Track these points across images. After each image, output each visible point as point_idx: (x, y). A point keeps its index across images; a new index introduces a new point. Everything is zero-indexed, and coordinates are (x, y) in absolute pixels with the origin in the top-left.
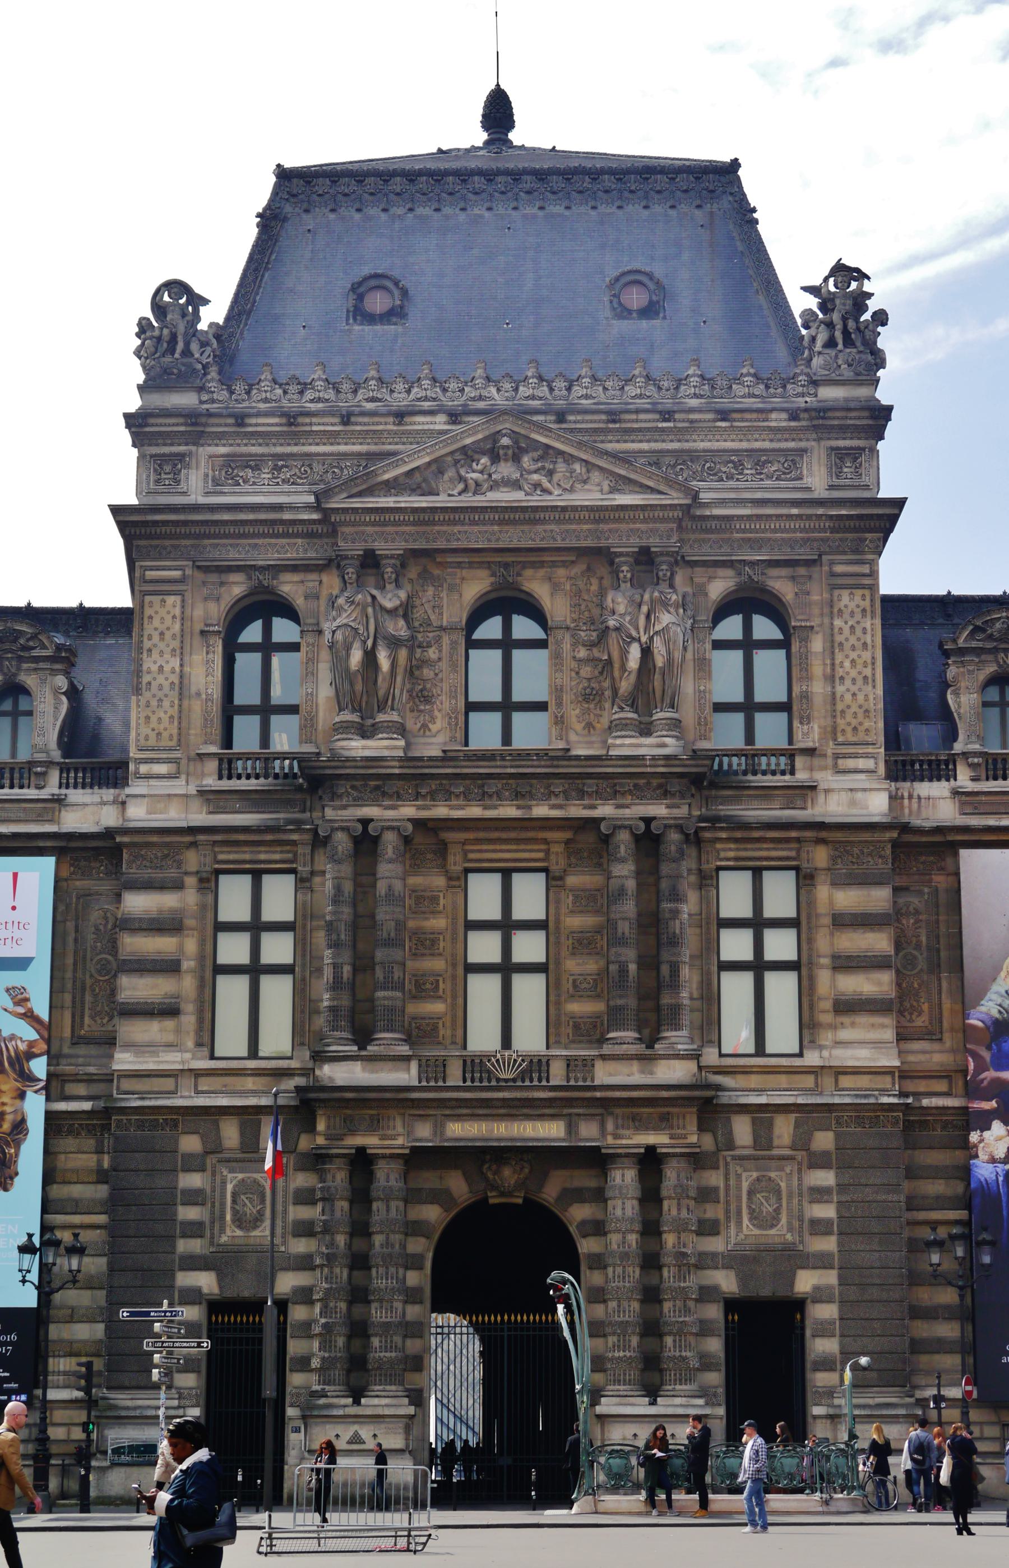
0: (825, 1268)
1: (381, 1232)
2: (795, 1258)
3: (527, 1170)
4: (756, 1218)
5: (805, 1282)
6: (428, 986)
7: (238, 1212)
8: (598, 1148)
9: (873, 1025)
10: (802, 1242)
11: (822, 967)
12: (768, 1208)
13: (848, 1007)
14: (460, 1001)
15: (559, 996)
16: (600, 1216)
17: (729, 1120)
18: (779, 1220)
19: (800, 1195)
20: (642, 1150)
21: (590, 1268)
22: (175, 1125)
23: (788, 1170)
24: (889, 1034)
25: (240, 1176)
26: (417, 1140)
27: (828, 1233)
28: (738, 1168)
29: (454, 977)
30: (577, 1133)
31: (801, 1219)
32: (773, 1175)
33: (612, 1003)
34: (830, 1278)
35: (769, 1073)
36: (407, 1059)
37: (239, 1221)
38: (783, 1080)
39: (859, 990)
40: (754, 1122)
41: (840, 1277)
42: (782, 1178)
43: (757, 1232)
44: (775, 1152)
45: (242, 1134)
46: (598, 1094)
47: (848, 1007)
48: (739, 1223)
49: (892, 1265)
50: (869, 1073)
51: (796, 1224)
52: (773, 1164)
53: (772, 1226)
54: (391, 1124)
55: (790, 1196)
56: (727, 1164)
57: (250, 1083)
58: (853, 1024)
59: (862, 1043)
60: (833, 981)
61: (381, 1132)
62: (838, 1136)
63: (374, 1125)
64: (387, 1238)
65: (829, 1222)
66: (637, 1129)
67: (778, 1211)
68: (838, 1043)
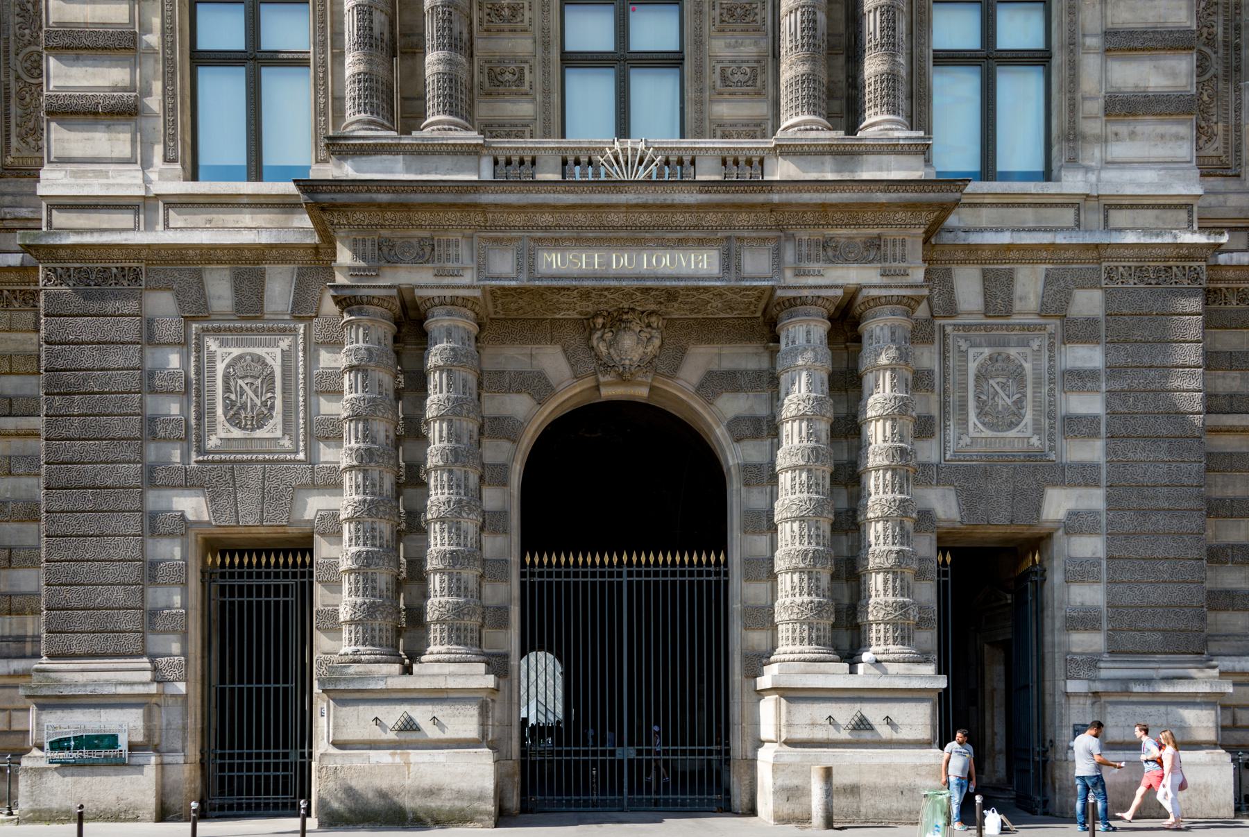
0: (1086, 485)
2: (1043, 470)
3: (657, 342)
4: (986, 415)
5: (1057, 504)
6: (508, 76)
7: (233, 404)
9: (1162, 137)
10: (1052, 448)
11: (1087, 51)
12: (1004, 400)
13: (1125, 107)
14: (556, 98)
15: (701, 91)
16: (762, 411)
17: (948, 273)
18: (1020, 417)
19: (1051, 381)
21: (747, 484)
22: (136, 275)
23: (1035, 345)
24: (1185, 150)
25: (236, 351)
27: (1095, 435)
28: (962, 342)
29: (546, 63)
31: (1051, 416)
32: (1013, 352)
34: (1095, 499)
35: (1007, 205)
37: (234, 420)
38: (1028, 216)
39: (1142, 84)
40: (985, 273)
41: (1109, 499)
42: (1027, 359)
43: (988, 433)
44: (1015, 320)
45: (237, 290)
47: (1125, 107)
48: (964, 422)
49: (1186, 481)
50: (1154, 207)
51: (1046, 423)
52: (1014, 335)
53: (1011, 425)
55: (1038, 383)
56: (945, 336)
57: (246, 218)
58: (1133, 135)
59: (1145, 163)
60: (1104, 70)
62: (1109, 296)
65: (1093, 420)
67: (1019, 403)
68: (1109, 164)
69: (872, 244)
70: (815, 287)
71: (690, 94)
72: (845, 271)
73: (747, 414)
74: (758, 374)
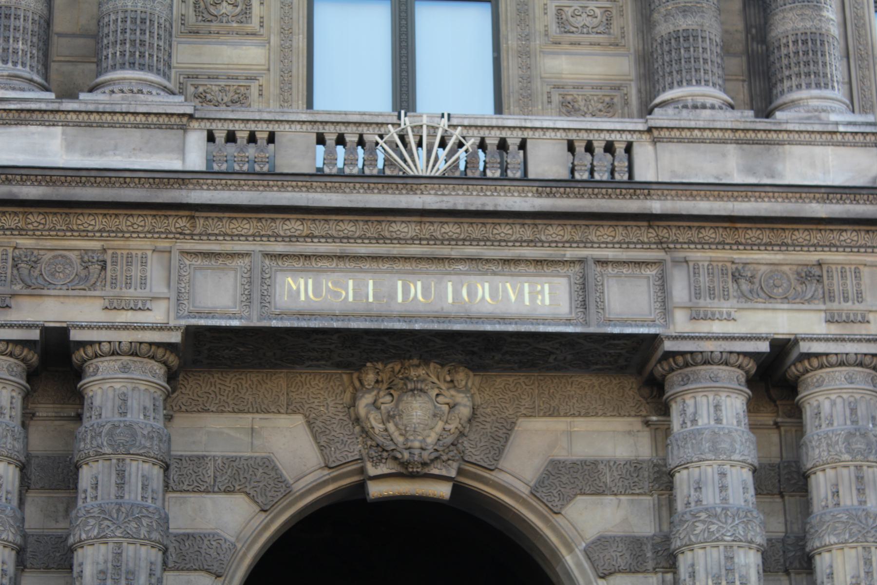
1: (102, 538)
3: (465, 411)
8: (654, 340)
14: (300, 42)
15: (527, 38)
20: (764, 347)
26: (200, 314)
30: (601, 306)
33: (663, 29)
36: (182, 122)
46: (656, 206)
54: (136, 272)
61: (109, 292)
63: (93, 273)
64: (118, 555)
66: (743, 296)
69: (809, 275)
70: (725, 338)
71: (511, 41)
72: (769, 314)
73: (619, 532)
74: (635, 466)
